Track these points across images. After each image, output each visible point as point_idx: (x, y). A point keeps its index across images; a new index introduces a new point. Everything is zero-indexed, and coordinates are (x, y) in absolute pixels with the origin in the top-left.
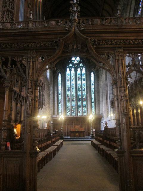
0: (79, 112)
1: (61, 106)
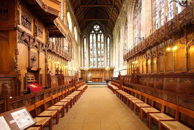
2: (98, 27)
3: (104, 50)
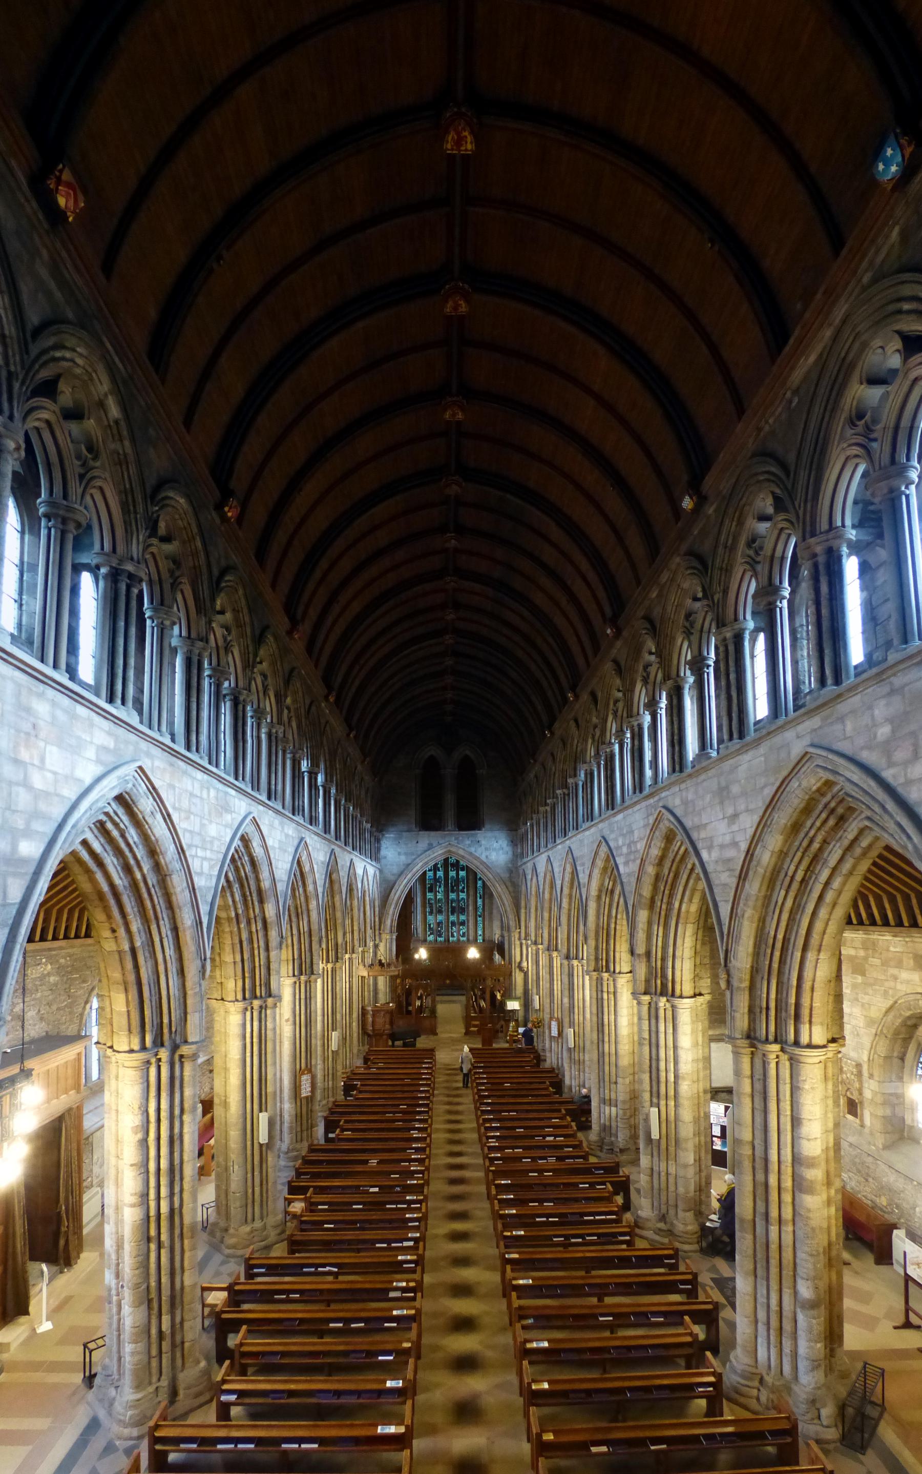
0: (453, 936)
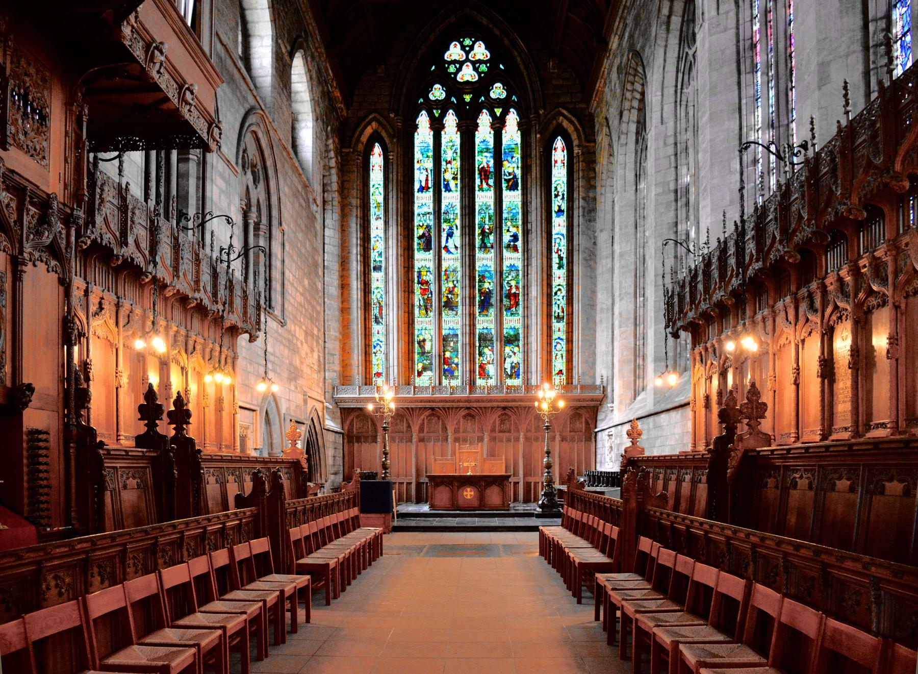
0: (483, 374)
1: (387, 335)
2: (480, 51)
3: (526, 242)
